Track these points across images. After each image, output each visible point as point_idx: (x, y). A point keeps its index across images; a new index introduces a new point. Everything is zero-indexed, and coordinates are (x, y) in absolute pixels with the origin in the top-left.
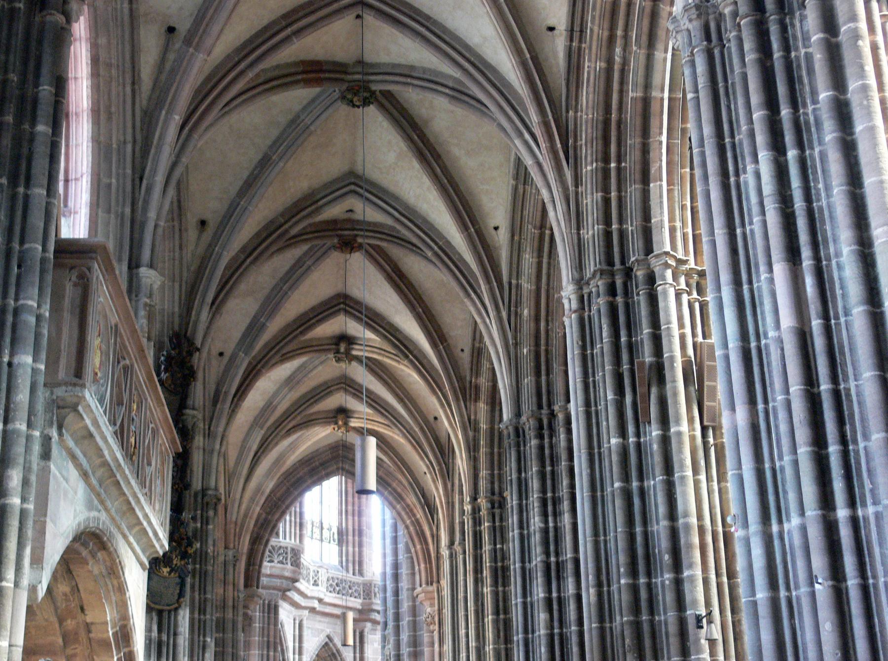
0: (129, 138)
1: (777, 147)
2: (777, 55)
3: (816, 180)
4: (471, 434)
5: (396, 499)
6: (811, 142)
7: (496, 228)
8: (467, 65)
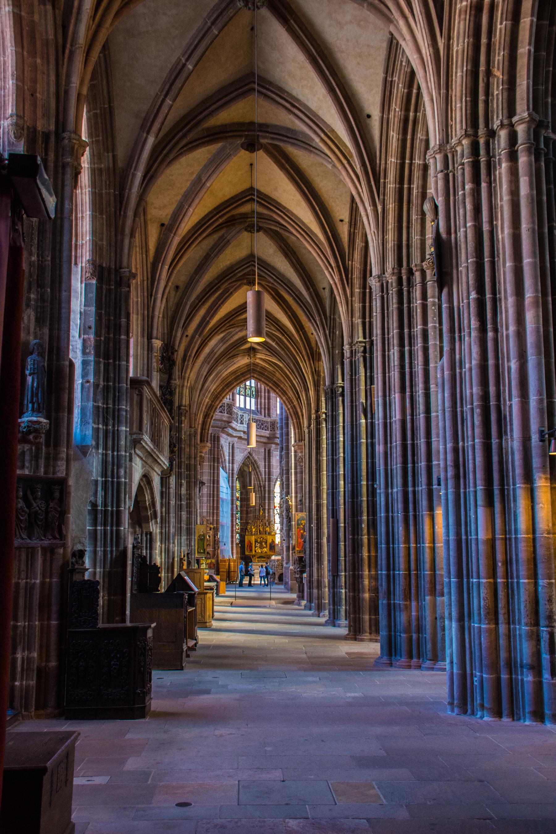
0: (145, 278)
1: (401, 345)
2: (405, 305)
3: (415, 360)
4: (316, 377)
5: (282, 393)
6: (414, 343)
7: (324, 289)
8: (303, 233)
